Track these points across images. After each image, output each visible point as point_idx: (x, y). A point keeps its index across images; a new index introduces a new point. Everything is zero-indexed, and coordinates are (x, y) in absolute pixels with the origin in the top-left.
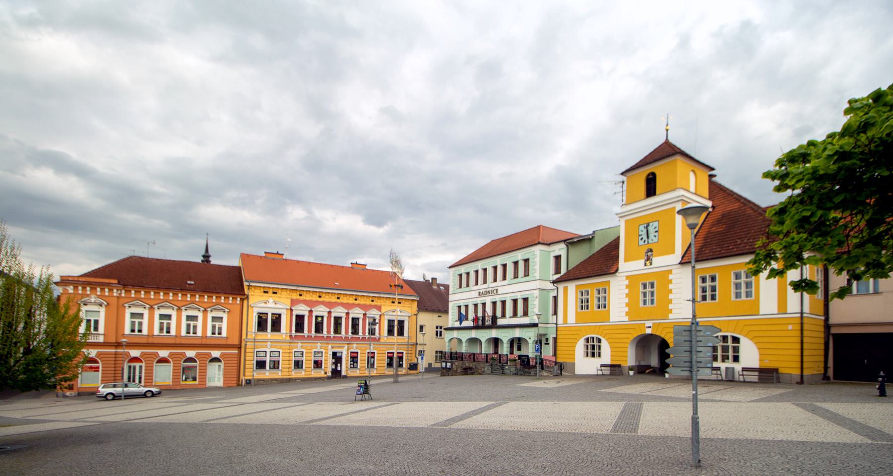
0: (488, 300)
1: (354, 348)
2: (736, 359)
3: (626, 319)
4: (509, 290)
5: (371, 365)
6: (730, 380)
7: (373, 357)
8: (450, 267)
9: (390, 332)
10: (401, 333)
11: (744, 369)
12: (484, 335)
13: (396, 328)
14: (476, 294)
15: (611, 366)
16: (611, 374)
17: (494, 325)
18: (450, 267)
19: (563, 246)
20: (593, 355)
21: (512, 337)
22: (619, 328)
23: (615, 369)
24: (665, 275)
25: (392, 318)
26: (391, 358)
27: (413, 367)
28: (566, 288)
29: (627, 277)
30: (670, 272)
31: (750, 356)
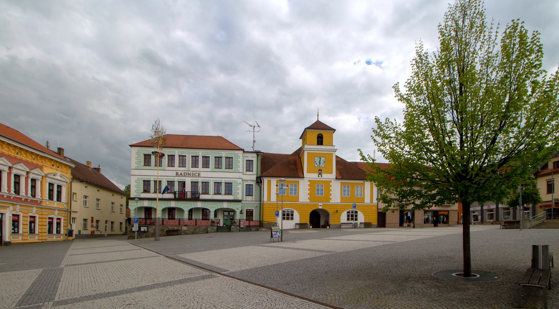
0: (188, 181)
1: (34, 211)
2: (356, 220)
3: (309, 201)
4: (211, 175)
5: (32, 231)
6: (355, 226)
7: (34, 222)
8: (131, 146)
9: (51, 197)
10: (59, 199)
11: (361, 223)
12: (186, 206)
13: (54, 192)
14: (174, 174)
15: (300, 224)
16: (300, 228)
17: (195, 198)
18: (131, 146)
19: (255, 155)
20: (288, 219)
21: (191, 208)
22: (303, 205)
23: (302, 226)
24: (327, 183)
25: (52, 181)
26: (51, 224)
27: (70, 233)
28: (269, 182)
29: (309, 181)
30: (331, 182)
31: (361, 218)
